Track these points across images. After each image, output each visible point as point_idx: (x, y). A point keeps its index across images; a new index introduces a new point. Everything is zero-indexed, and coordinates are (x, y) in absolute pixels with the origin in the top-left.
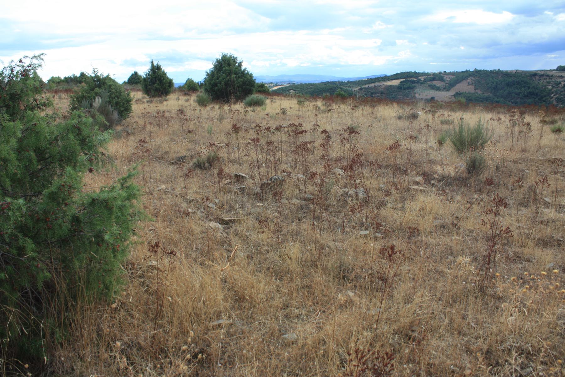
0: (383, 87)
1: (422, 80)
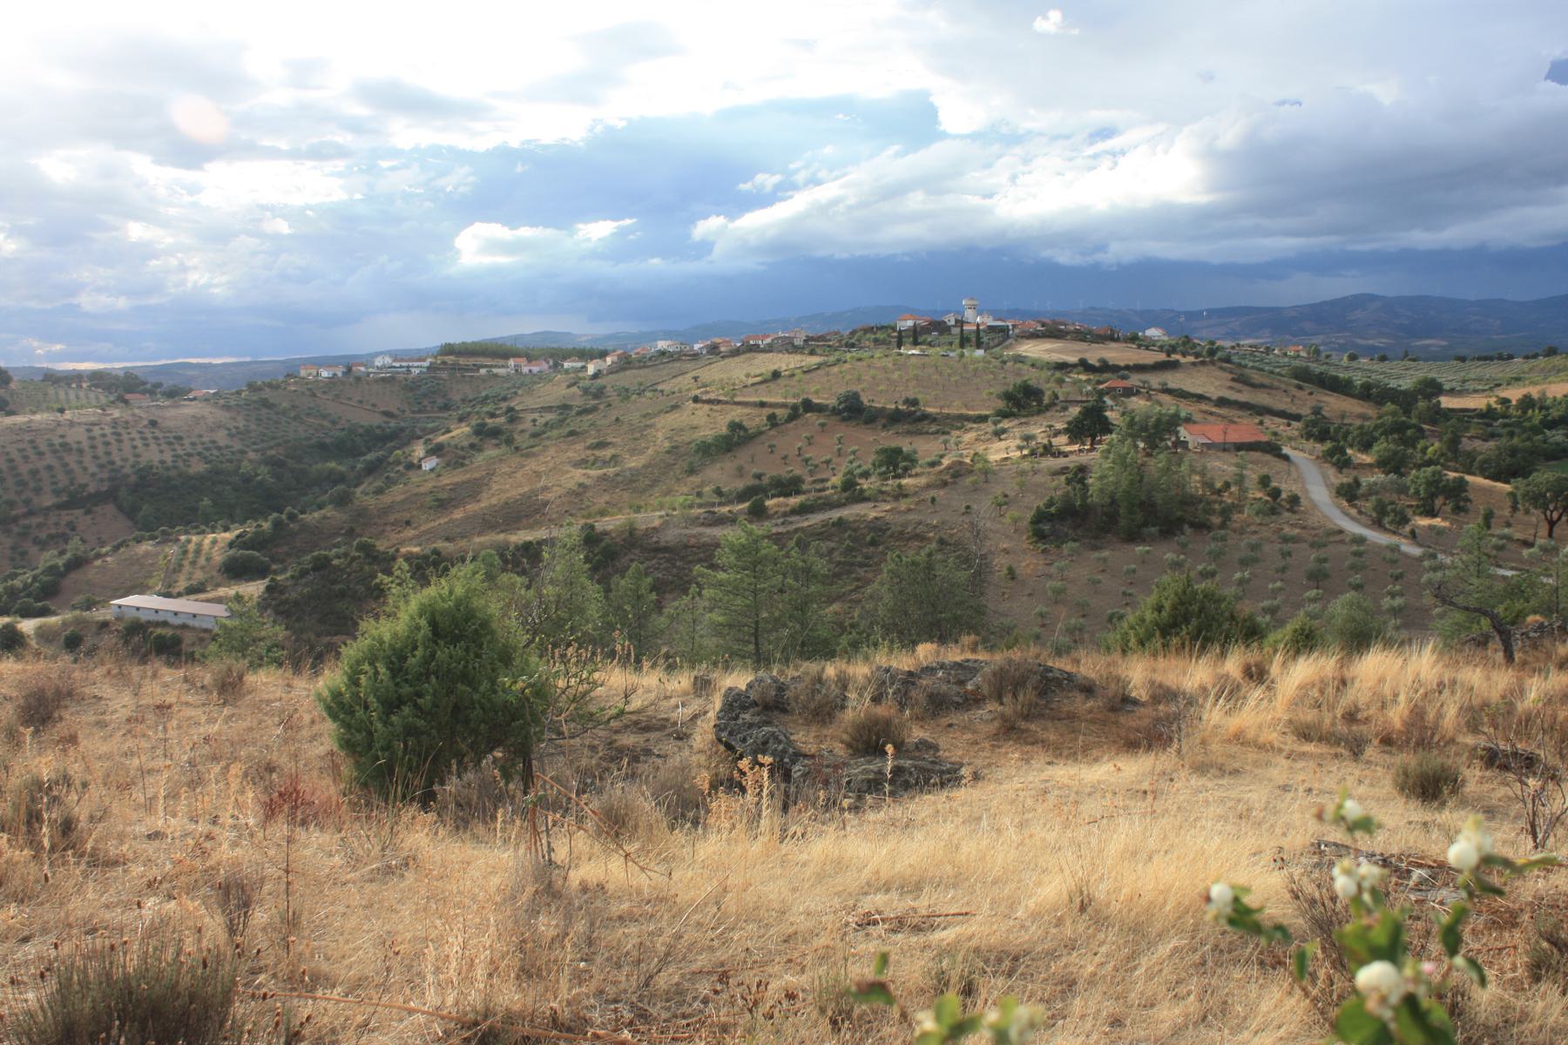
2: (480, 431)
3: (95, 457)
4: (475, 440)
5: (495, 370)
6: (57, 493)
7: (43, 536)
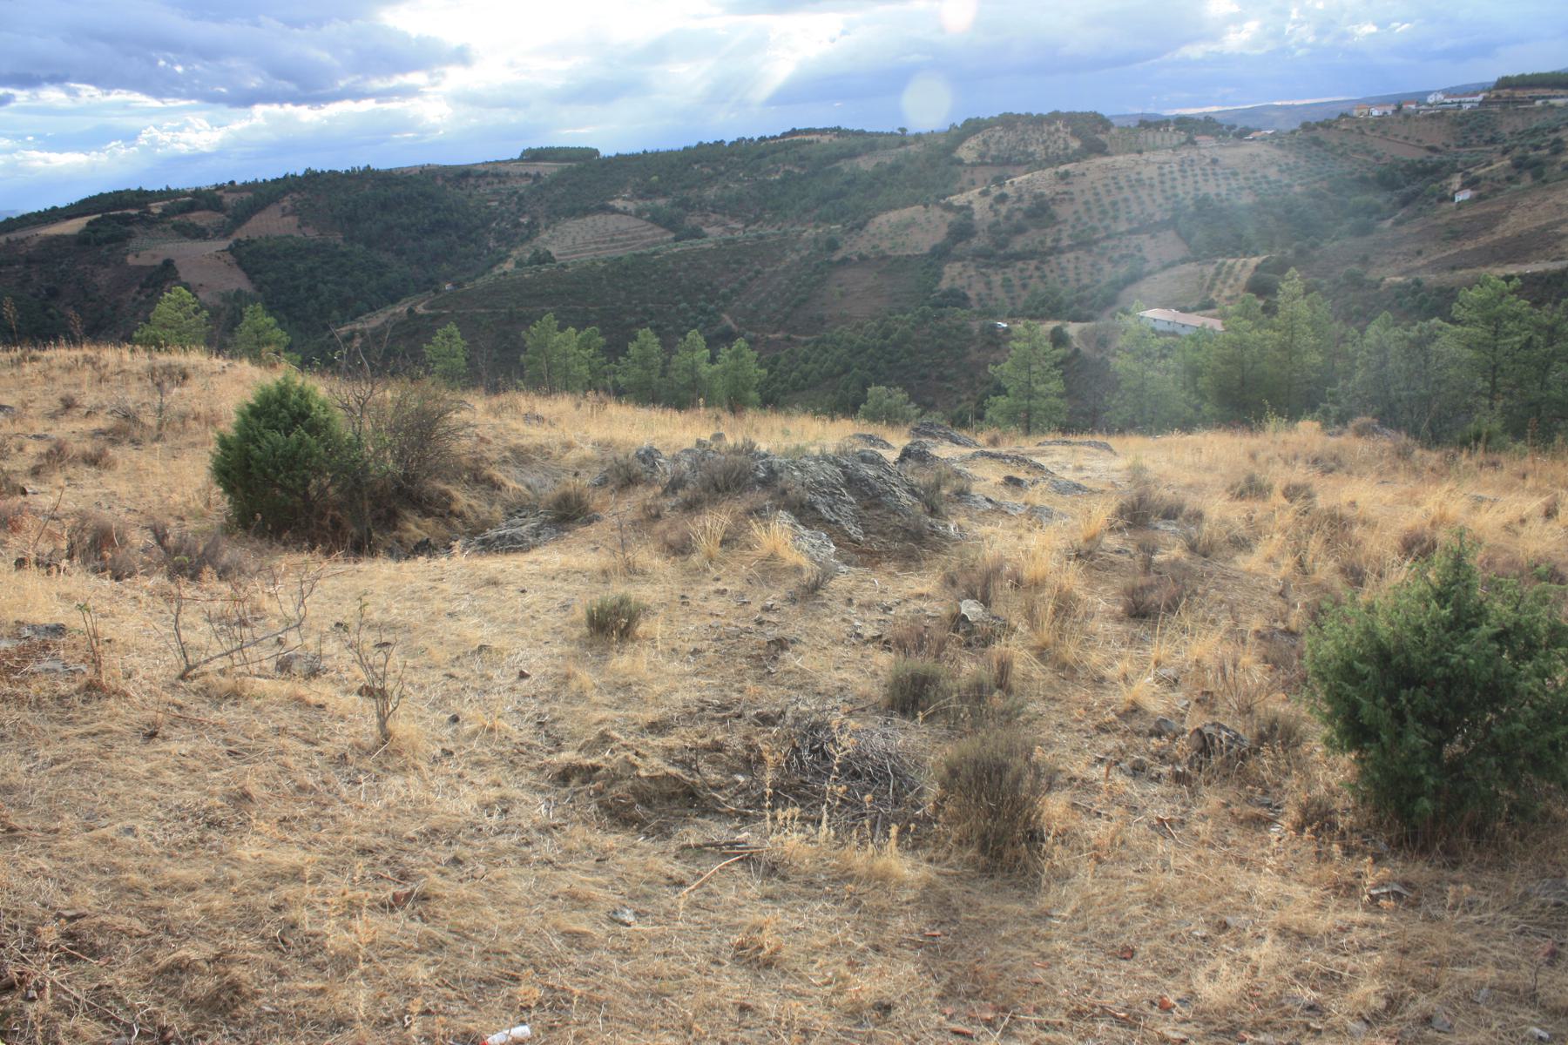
0: (36, 241)
1: (157, 211)
2: (1520, 165)
3: (1163, 191)
4: (1513, 173)
5: (1552, 101)
6: (1130, 221)
7: (1116, 256)
